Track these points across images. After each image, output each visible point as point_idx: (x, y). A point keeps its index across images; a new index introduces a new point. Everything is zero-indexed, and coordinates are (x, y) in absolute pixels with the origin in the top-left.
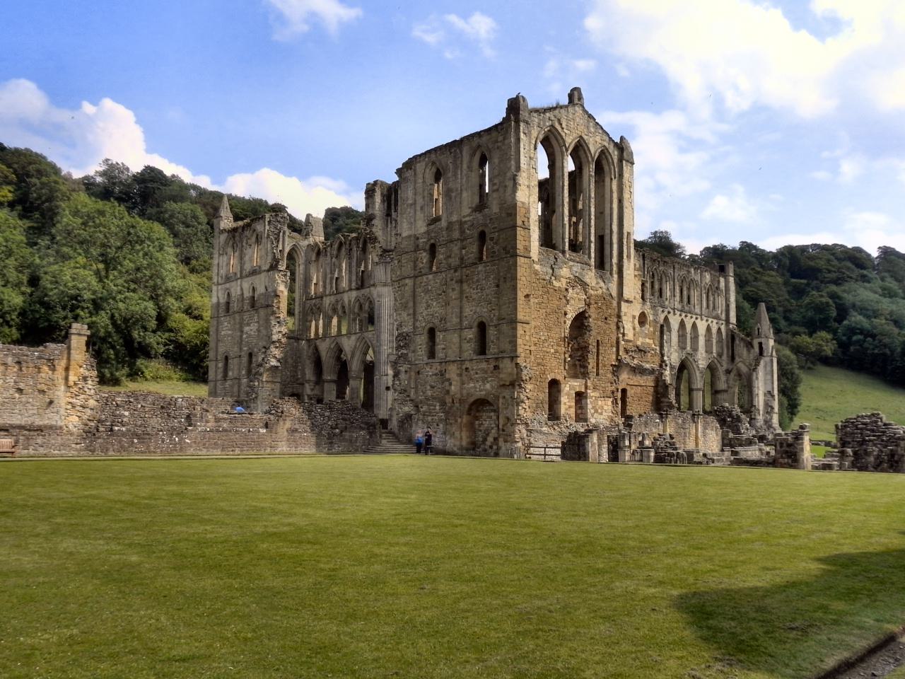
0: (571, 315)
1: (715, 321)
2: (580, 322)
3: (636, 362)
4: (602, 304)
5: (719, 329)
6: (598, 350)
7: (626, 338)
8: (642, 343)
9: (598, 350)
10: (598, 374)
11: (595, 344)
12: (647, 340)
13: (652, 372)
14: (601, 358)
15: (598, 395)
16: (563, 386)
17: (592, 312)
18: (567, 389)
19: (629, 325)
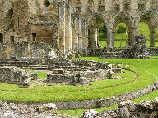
0: (6, 11)
2: (11, 12)
3: (37, 22)
4: (20, 4)
6: (19, 20)
7: (30, 13)
8: (45, 13)
9: (19, 20)
10: (19, 29)
11: (17, 19)
12: (49, 12)
13: (50, 24)
14: (20, 23)
15: (19, 37)
16: (3, 35)
17: (15, 8)
18: (6, 36)
19: (33, 10)
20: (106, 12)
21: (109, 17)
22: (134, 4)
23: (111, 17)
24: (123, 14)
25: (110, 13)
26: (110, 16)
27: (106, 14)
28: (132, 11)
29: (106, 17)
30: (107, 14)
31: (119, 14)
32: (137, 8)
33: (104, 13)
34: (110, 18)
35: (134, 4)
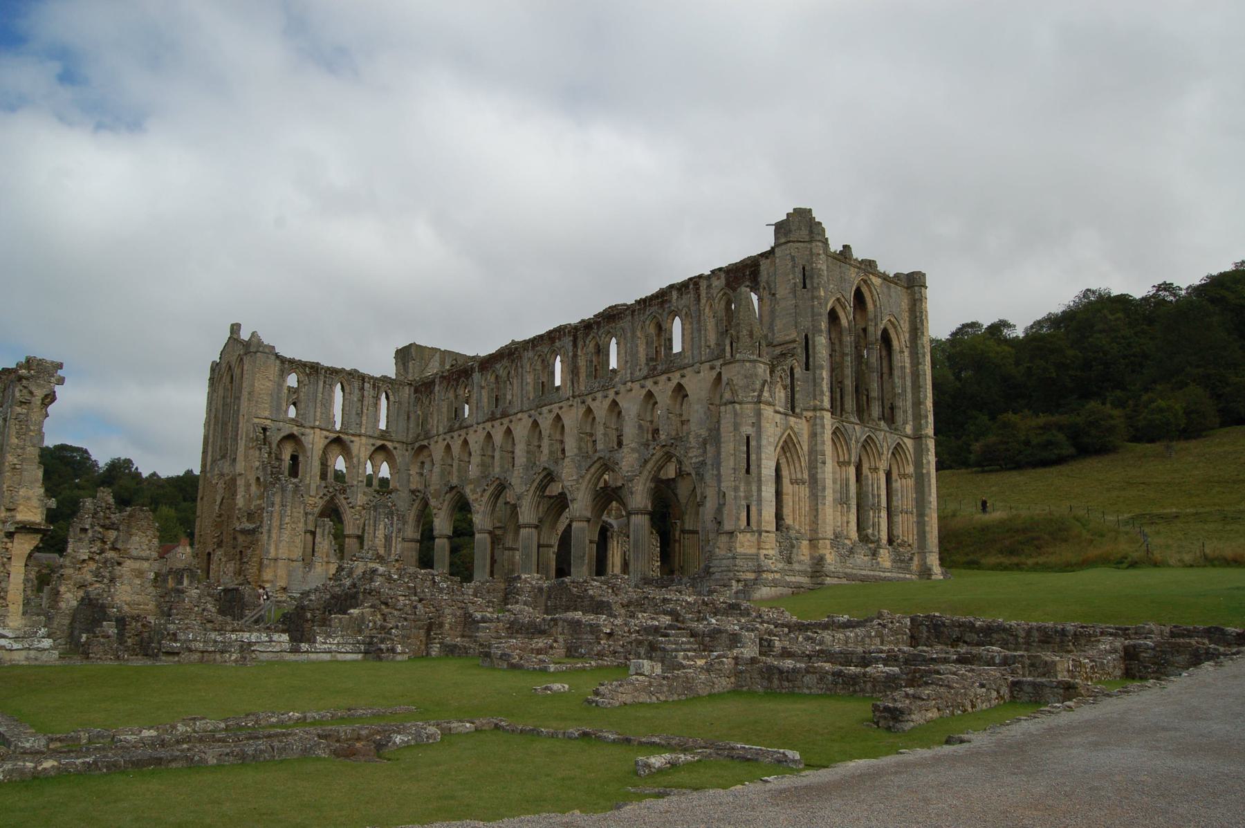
21: (475, 496)
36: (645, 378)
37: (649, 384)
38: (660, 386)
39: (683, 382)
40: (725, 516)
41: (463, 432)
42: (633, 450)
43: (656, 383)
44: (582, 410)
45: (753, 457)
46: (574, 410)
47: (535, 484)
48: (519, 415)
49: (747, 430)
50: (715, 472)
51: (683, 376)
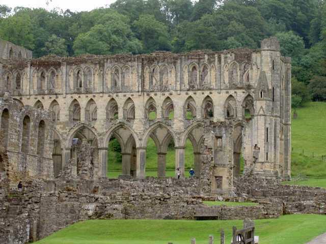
1: (240, 92)
5: (249, 95)
20: (60, 123)
21: (65, 131)
22: (102, 112)
23: (68, 130)
24: (86, 126)
25: (65, 124)
26: (66, 130)
27: (60, 126)
28: (97, 122)
29: (61, 131)
30: (62, 126)
31: (80, 126)
32: (105, 117)
33: (57, 124)
34: (66, 133)
35: (102, 112)
36: (189, 90)
37: (191, 93)
38: (197, 95)
39: (210, 95)
40: (260, 156)
41: (54, 97)
42: (181, 121)
43: (195, 94)
44: (147, 98)
45: (269, 135)
46: (142, 98)
47: (112, 129)
48: (101, 95)
49: (268, 126)
50: (250, 139)
51: (211, 93)
